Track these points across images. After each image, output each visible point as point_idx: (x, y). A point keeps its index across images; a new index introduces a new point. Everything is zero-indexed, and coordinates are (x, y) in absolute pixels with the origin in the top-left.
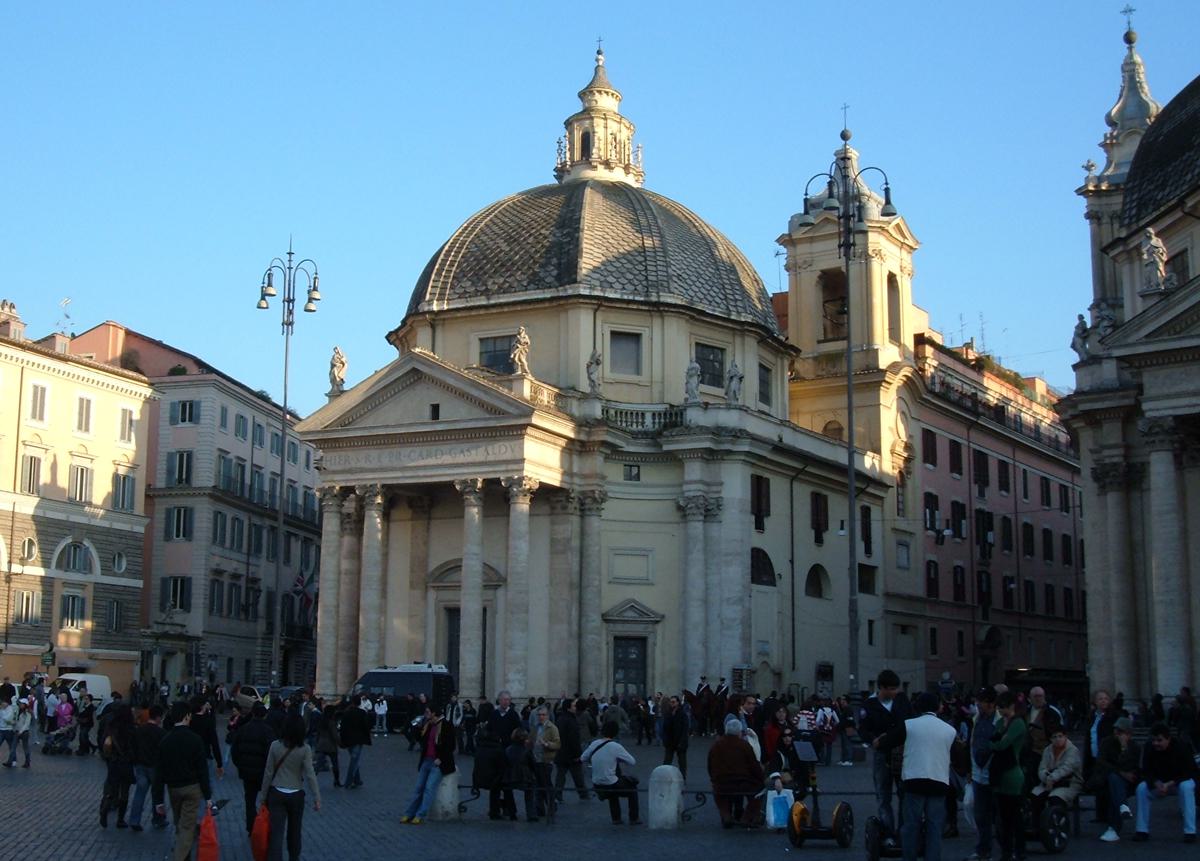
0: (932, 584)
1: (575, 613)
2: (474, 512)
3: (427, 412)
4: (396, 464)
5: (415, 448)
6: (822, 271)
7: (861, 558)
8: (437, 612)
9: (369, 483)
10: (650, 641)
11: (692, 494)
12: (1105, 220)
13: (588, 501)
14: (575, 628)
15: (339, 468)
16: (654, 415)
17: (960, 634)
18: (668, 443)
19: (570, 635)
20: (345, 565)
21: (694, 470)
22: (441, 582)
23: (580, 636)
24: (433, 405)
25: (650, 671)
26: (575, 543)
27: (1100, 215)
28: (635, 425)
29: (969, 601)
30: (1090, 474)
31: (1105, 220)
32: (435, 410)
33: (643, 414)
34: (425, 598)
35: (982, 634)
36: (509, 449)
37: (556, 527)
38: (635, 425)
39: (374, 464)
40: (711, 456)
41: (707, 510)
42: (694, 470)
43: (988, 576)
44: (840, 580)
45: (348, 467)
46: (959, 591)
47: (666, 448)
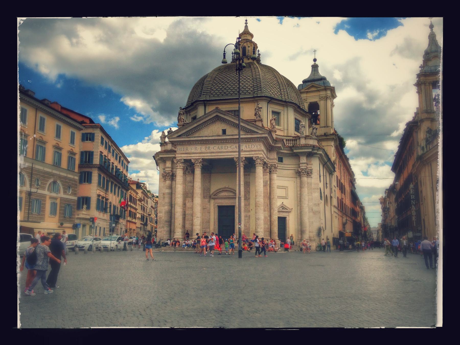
3: (221, 133)
4: (208, 151)
5: (216, 145)
6: (310, 103)
8: (214, 208)
9: (198, 158)
11: (303, 167)
13: (273, 168)
15: (184, 152)
18: (296, 149)
20: (167, 191)
21: (303, 160)
22: (216, 196)
26: (269, 183)
32: (224, 132)
34: (209, 202)
36: (255, 146)
39: (199, 151)
40: (310, 155)
41: (308, 173)
42: (303, 160)
45: (187, 152)
47: (295, 151)
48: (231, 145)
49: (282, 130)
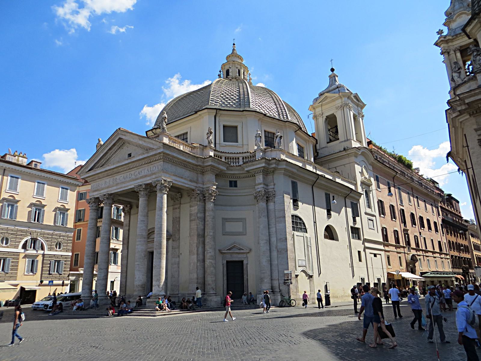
0: (385, 237)
1: (200, 249)
2: (142, 201)
7: (351, 224)
10: (245, 262)
12: (452, 52)
14: (201, 257)
16: (243, 158)
17: (400, 257)
19: (198, 260)
23: (204, 261)
24: (129, 154)
25: (245, 276)
27: (449, 51)
28: (235, 163)
29: (401, 244)
30: (477, 144)
31: (452, 52)
33: (238, 158)
35: (409, 257)
37: (192, 208)
38: (235, 163)
43: (408, 235)
44: (342, 232)
46: (397, 240)
48: (134, 172)
49: (240, 146)
